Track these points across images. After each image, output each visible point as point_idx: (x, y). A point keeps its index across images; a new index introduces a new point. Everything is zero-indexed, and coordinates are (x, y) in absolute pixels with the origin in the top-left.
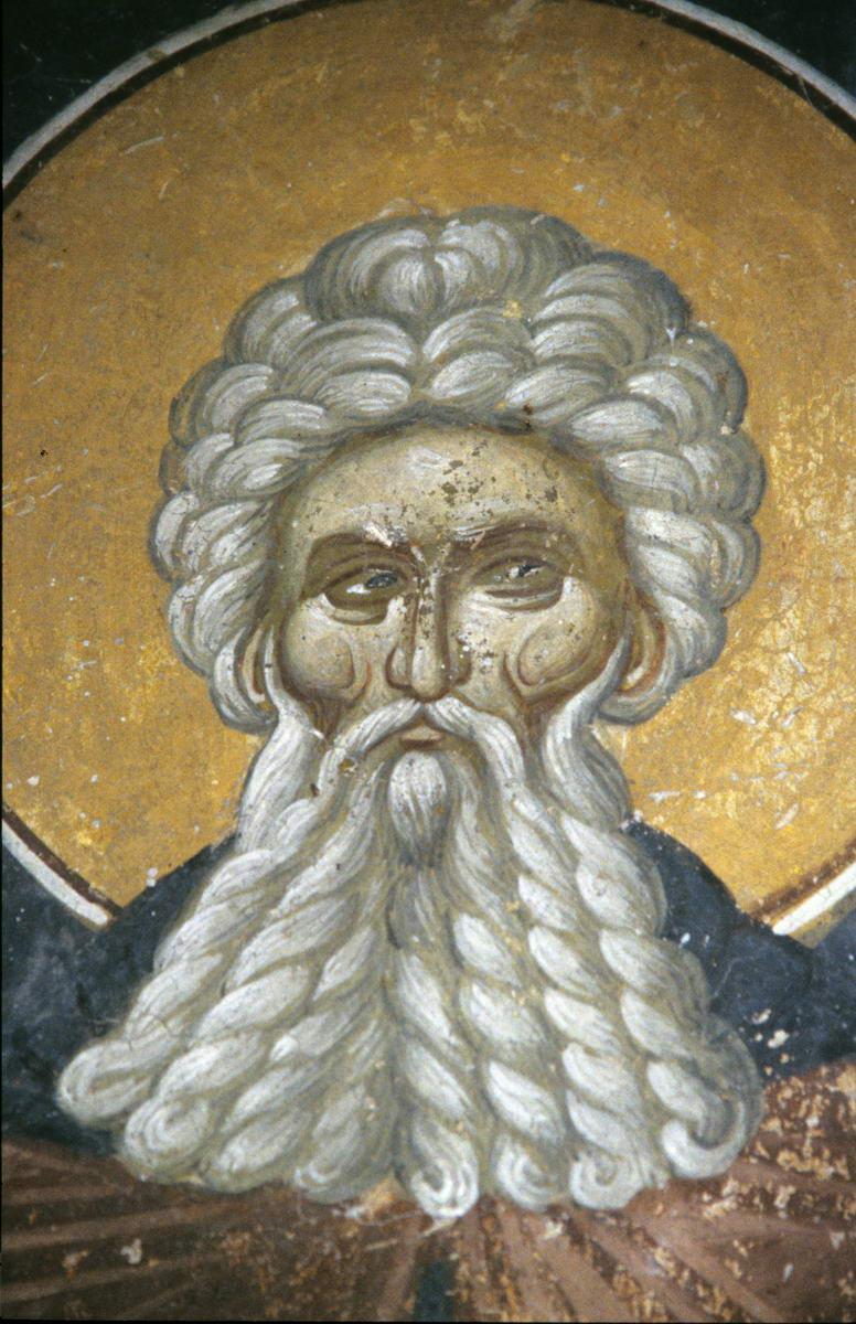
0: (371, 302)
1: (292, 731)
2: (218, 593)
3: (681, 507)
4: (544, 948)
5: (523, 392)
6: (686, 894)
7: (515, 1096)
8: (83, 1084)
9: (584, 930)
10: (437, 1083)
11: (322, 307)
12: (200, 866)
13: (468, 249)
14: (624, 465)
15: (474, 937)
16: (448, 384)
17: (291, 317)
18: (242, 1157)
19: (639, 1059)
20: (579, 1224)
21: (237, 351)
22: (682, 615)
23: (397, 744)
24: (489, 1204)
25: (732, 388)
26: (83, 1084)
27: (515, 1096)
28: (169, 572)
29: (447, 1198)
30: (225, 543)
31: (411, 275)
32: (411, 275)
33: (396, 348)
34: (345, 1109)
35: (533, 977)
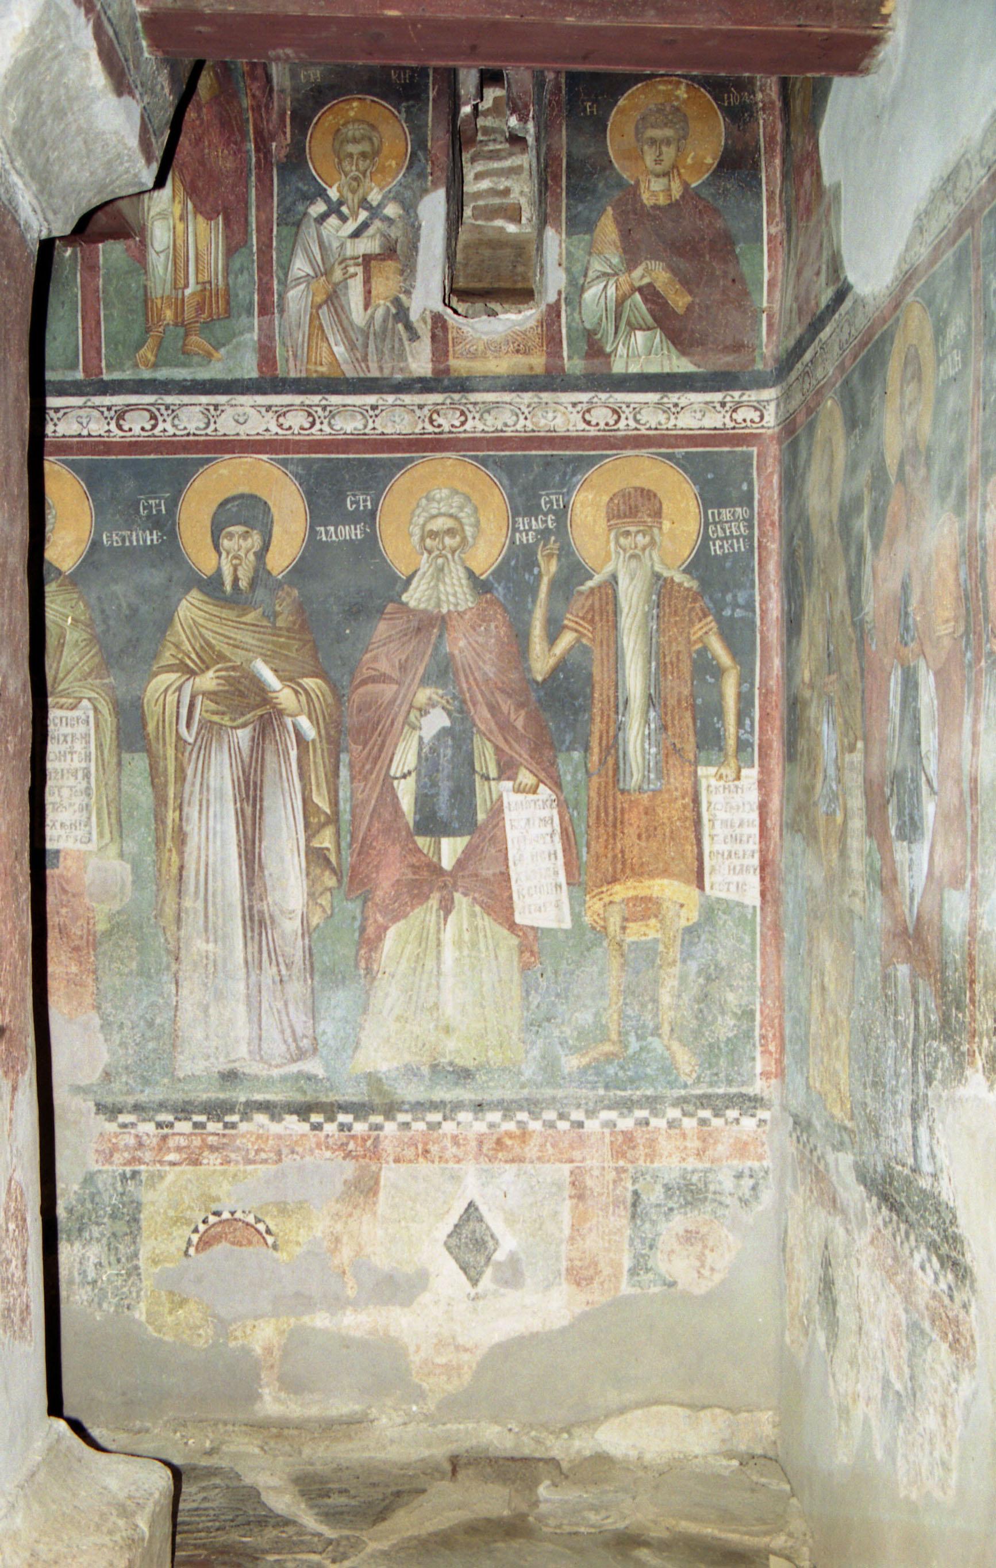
0: (433, 499)
1: (426, 555)
2: (416, 539)
3: (471, 525)
4: (455, 581)
5: (452, 511)
6: (471, 574)
7: (452, 599)
8: (404, 598)
9: (459, 579)
10: (443, 598)
11: (428, 500)
12: (416, 572)
13: (445, 492)
14: (464, 521)
15: (447, 580)
16: (443, 510)
17: (424, 502)
18: (422, 606)
19: (465, 594)
20: (459, 613)
21: (418, 506)
22: (470, 539)
23: (438, 556)
24: (449, 611)
25: (476, 510)
26: (404, 598)
27: (452, 599)
28: (411, 535)
29: (444, 610)
30: (417, 531)
31: (438, 496)
32: (438, 496)
33: (436, 505)
34: (433, 603)
35: (453, 585)
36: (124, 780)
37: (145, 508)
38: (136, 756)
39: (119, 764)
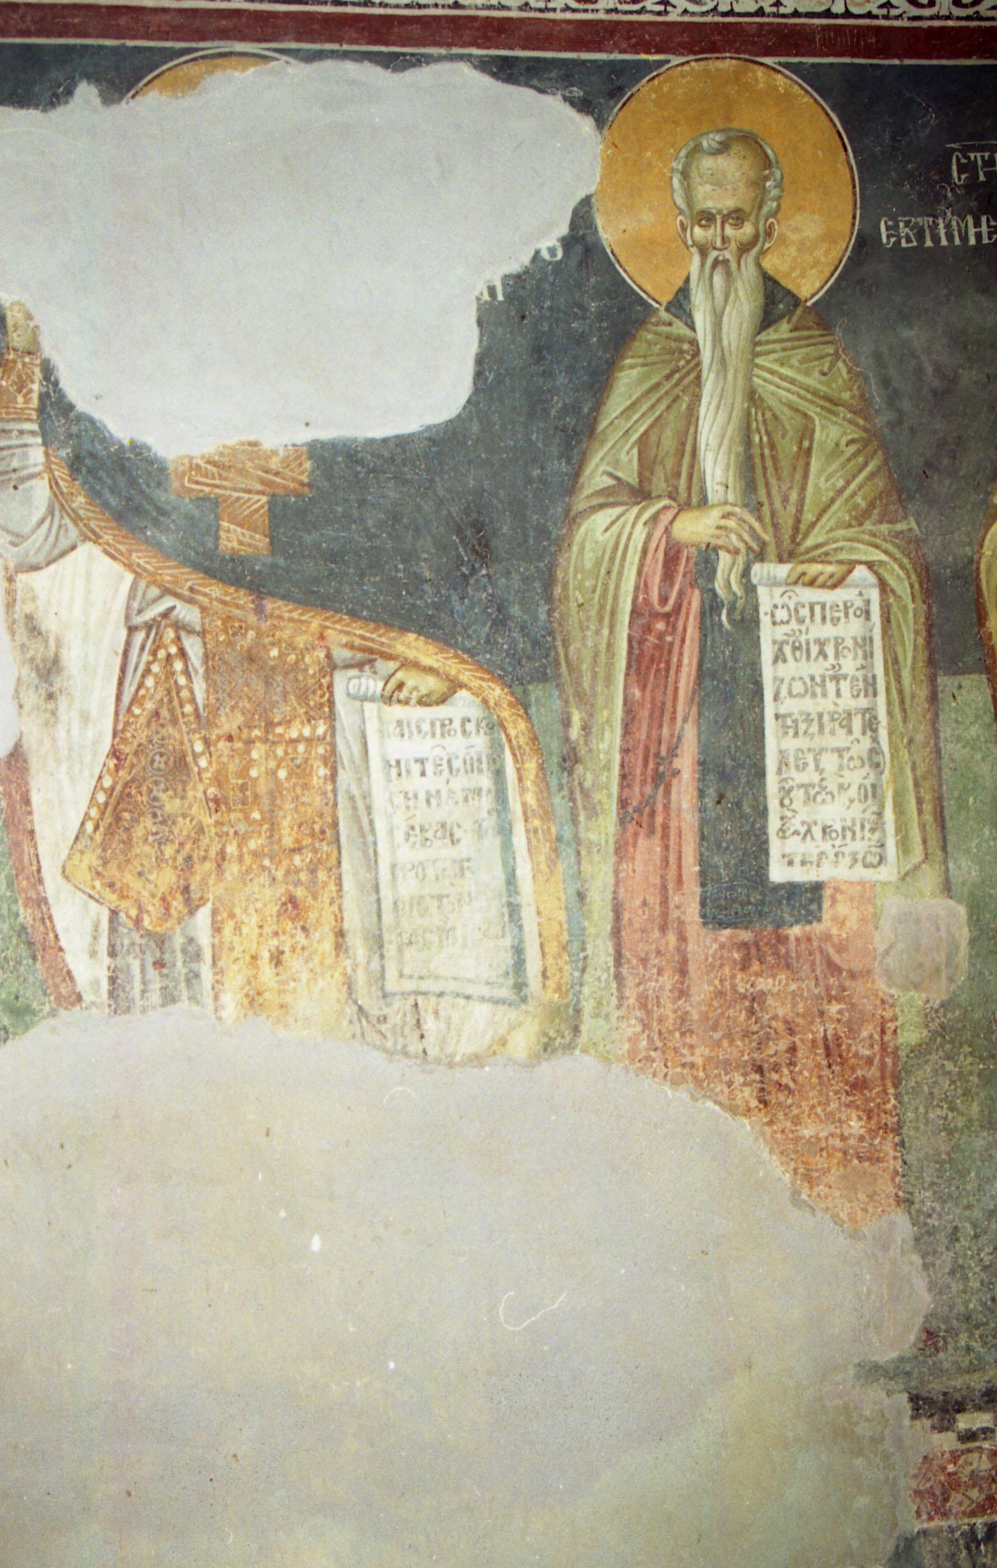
36: (946, 732)
37: (962, 169)
38: (967, 681)
39: (933, 698)
